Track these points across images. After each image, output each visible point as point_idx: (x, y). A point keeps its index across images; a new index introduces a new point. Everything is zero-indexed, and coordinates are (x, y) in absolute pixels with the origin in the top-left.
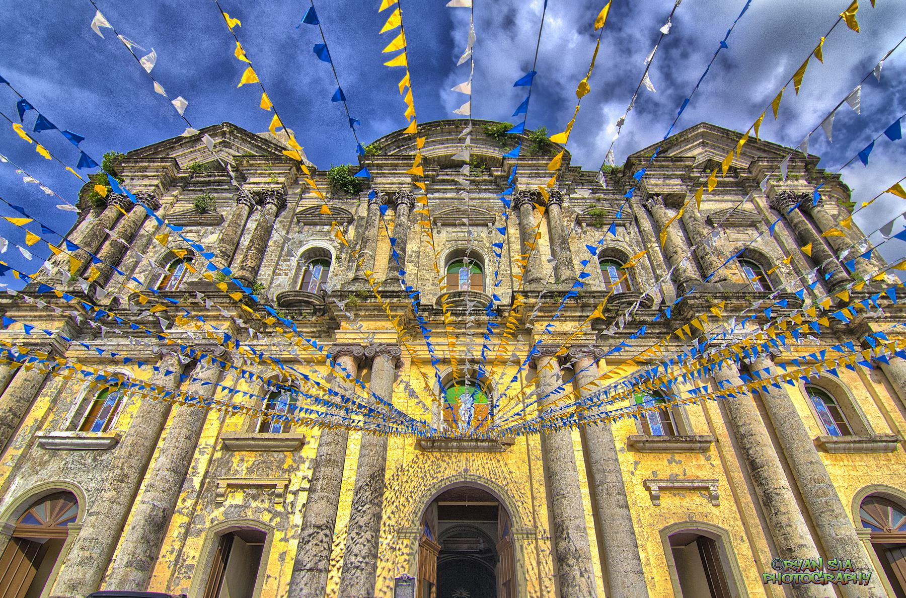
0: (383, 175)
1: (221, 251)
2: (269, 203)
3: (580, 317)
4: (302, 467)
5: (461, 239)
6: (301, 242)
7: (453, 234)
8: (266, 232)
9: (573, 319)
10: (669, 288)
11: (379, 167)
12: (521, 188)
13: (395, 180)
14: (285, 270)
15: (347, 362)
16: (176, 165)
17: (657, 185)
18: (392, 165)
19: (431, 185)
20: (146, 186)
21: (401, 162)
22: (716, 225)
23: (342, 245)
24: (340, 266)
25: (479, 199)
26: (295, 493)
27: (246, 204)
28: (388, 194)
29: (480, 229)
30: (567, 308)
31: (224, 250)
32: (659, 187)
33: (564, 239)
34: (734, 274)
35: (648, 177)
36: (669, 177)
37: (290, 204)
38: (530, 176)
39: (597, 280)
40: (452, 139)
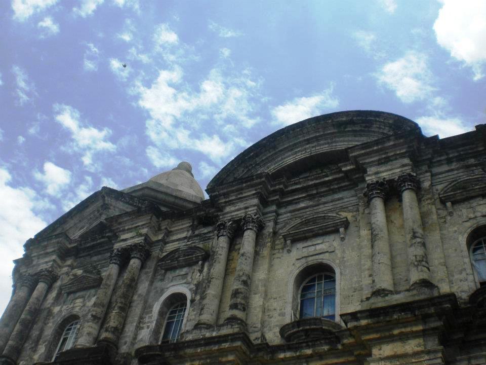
0: (230, 203)
1: (92, 316)
2: (133, 257)
3: (423, 331)
7: (305, 250)
8: (132, 285)
9: (415, 335)
11: (226, 195)
13: (241, 205)
14: (149, 322)
16: (67, 237)
18: (237, 190)
19: (282, 198)
20: (46, 262)
21: (244, 185)
23: (198, 285)
24: (193, 310)
27: (115, 263)
29: (331, 238)
30: (406, 323)
31: (94, 313)
38: (380, 163)
39: (464, 274)
40: (300, 142)
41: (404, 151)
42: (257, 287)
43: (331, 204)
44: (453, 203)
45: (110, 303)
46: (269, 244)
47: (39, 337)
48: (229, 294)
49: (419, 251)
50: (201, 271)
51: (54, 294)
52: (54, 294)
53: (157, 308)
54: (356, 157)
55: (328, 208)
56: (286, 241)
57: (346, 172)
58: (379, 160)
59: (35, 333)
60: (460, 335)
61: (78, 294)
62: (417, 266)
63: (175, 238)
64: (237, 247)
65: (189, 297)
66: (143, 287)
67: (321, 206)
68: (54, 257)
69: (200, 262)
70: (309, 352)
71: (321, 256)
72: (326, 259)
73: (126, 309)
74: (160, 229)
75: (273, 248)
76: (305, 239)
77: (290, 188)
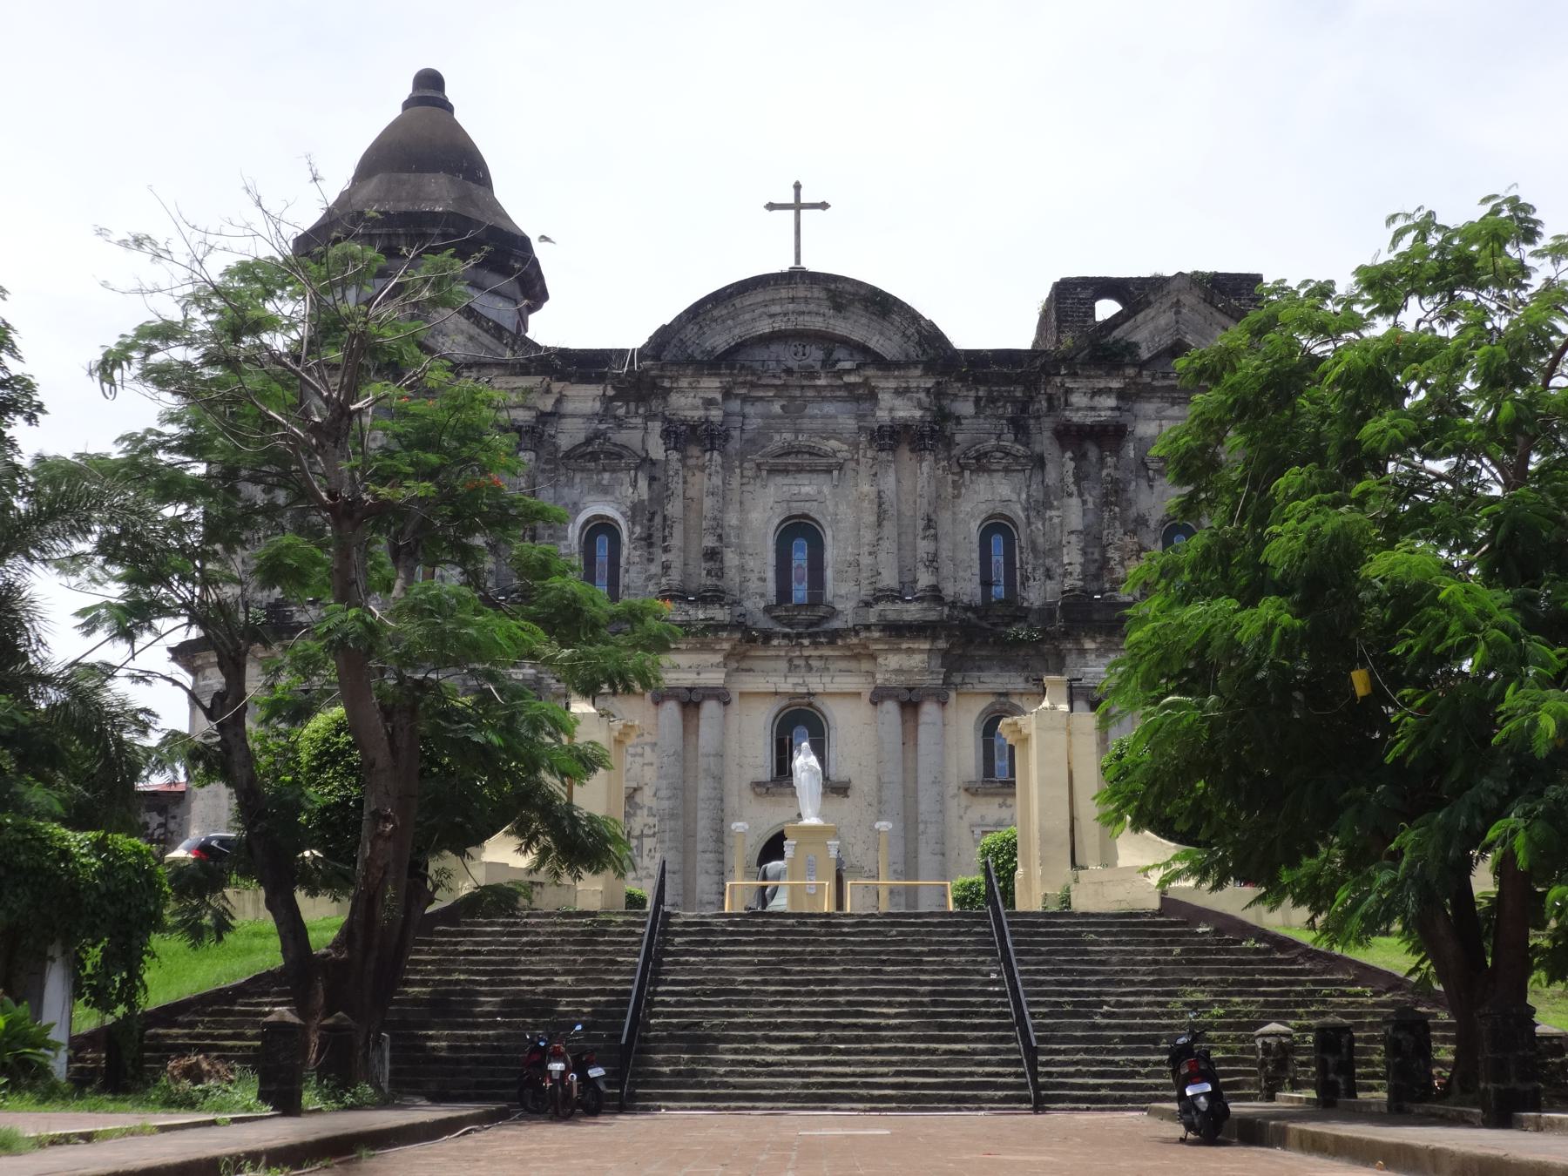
0: (680, 390)
3: (930, 650)
4: (639, 812)
5: (795, 498)
6: (575, 504)
7: (785, 488)
9: (921, 651)
12: (883, 415)
14: (566, 555)
17: (1078, 409)
22: (1151, 473)
25: (823, 417)
26: (641, 836)
28: (688, 425)
29: (823, 477)
30: (914, 638)
32: (1080, 414)
33: (929, 520)
35: (1069, 391)
38: (898, 392)
41: (929, 385)
42: (728, 536)
43: (820, 421)
44: (972, 472)
46: (738, 471)
49: (931, 548)
50: (634, 484)
54: (867, 379)
55: (814, 426)
56: (760, 470)
57: (847, 386)
58: (896, 389)
60: (960, 652)
62: (927, 567)
63: (569, 407)
64: (691, 462)
65: (622, 522)
67: (805, 420)
69: (632, 472)
70: (806, 642)
71: (808, 505)
72: (812, 509)
74: (548, 391)
75: (742, 477)
76: (785, 471)
77: (764, 381)
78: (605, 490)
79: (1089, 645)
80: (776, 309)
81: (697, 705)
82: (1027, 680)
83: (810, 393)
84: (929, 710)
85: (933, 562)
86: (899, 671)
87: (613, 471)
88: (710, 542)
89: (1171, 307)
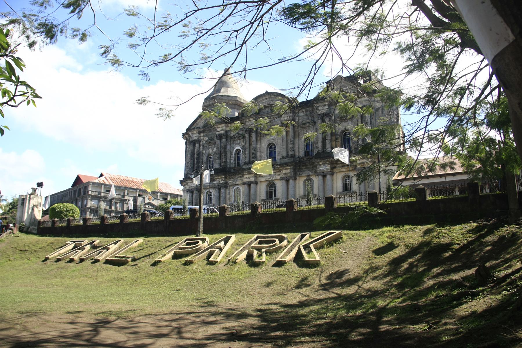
0: (247, 121)
8: (225, 147)
9: (289, 169)
10: (317, 150)
11: (245, 119)
15: (246, 186)
30: (286, 167)
34: (338, 141)
35: (318, 107)
36: (324, 105)
37: (229, 134)
45: (221, 152)
47: (203, 161)
48: (251, 154)
50: (243, 142)
51: (201, 147)
52: (201, 147)
53: (234, 153)
59: (201, 161)
61: (209, 147)
66: (228, 147)
68: (197, 134)
72: (273, 141)
73: (226, 155)
75: (261, 136)
78: (239, 144)
79: (321, 163)
80: (264, 101)
81: (250, 184)
82: (312, 172)
83: (272, 117)
84: (291, 182)
85: (293, 149)
86: (284, 174)
87: (240, 140)
88: (252, 151)
89: (339, 83)
